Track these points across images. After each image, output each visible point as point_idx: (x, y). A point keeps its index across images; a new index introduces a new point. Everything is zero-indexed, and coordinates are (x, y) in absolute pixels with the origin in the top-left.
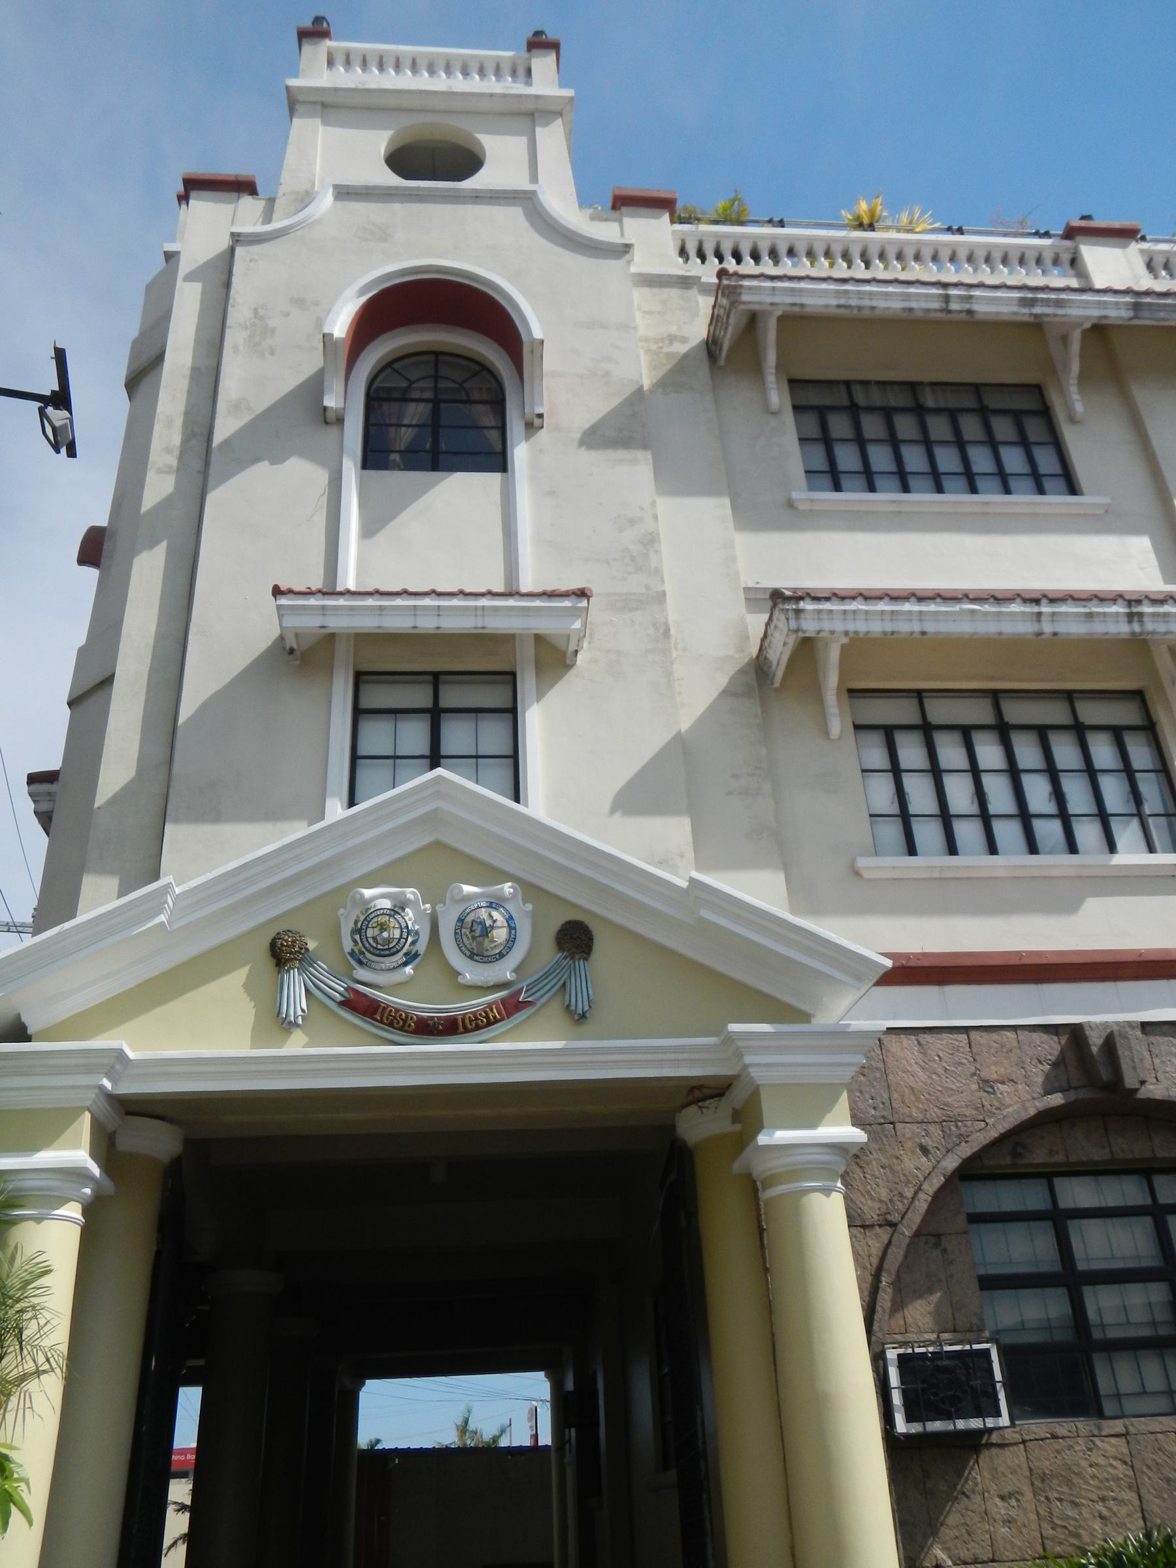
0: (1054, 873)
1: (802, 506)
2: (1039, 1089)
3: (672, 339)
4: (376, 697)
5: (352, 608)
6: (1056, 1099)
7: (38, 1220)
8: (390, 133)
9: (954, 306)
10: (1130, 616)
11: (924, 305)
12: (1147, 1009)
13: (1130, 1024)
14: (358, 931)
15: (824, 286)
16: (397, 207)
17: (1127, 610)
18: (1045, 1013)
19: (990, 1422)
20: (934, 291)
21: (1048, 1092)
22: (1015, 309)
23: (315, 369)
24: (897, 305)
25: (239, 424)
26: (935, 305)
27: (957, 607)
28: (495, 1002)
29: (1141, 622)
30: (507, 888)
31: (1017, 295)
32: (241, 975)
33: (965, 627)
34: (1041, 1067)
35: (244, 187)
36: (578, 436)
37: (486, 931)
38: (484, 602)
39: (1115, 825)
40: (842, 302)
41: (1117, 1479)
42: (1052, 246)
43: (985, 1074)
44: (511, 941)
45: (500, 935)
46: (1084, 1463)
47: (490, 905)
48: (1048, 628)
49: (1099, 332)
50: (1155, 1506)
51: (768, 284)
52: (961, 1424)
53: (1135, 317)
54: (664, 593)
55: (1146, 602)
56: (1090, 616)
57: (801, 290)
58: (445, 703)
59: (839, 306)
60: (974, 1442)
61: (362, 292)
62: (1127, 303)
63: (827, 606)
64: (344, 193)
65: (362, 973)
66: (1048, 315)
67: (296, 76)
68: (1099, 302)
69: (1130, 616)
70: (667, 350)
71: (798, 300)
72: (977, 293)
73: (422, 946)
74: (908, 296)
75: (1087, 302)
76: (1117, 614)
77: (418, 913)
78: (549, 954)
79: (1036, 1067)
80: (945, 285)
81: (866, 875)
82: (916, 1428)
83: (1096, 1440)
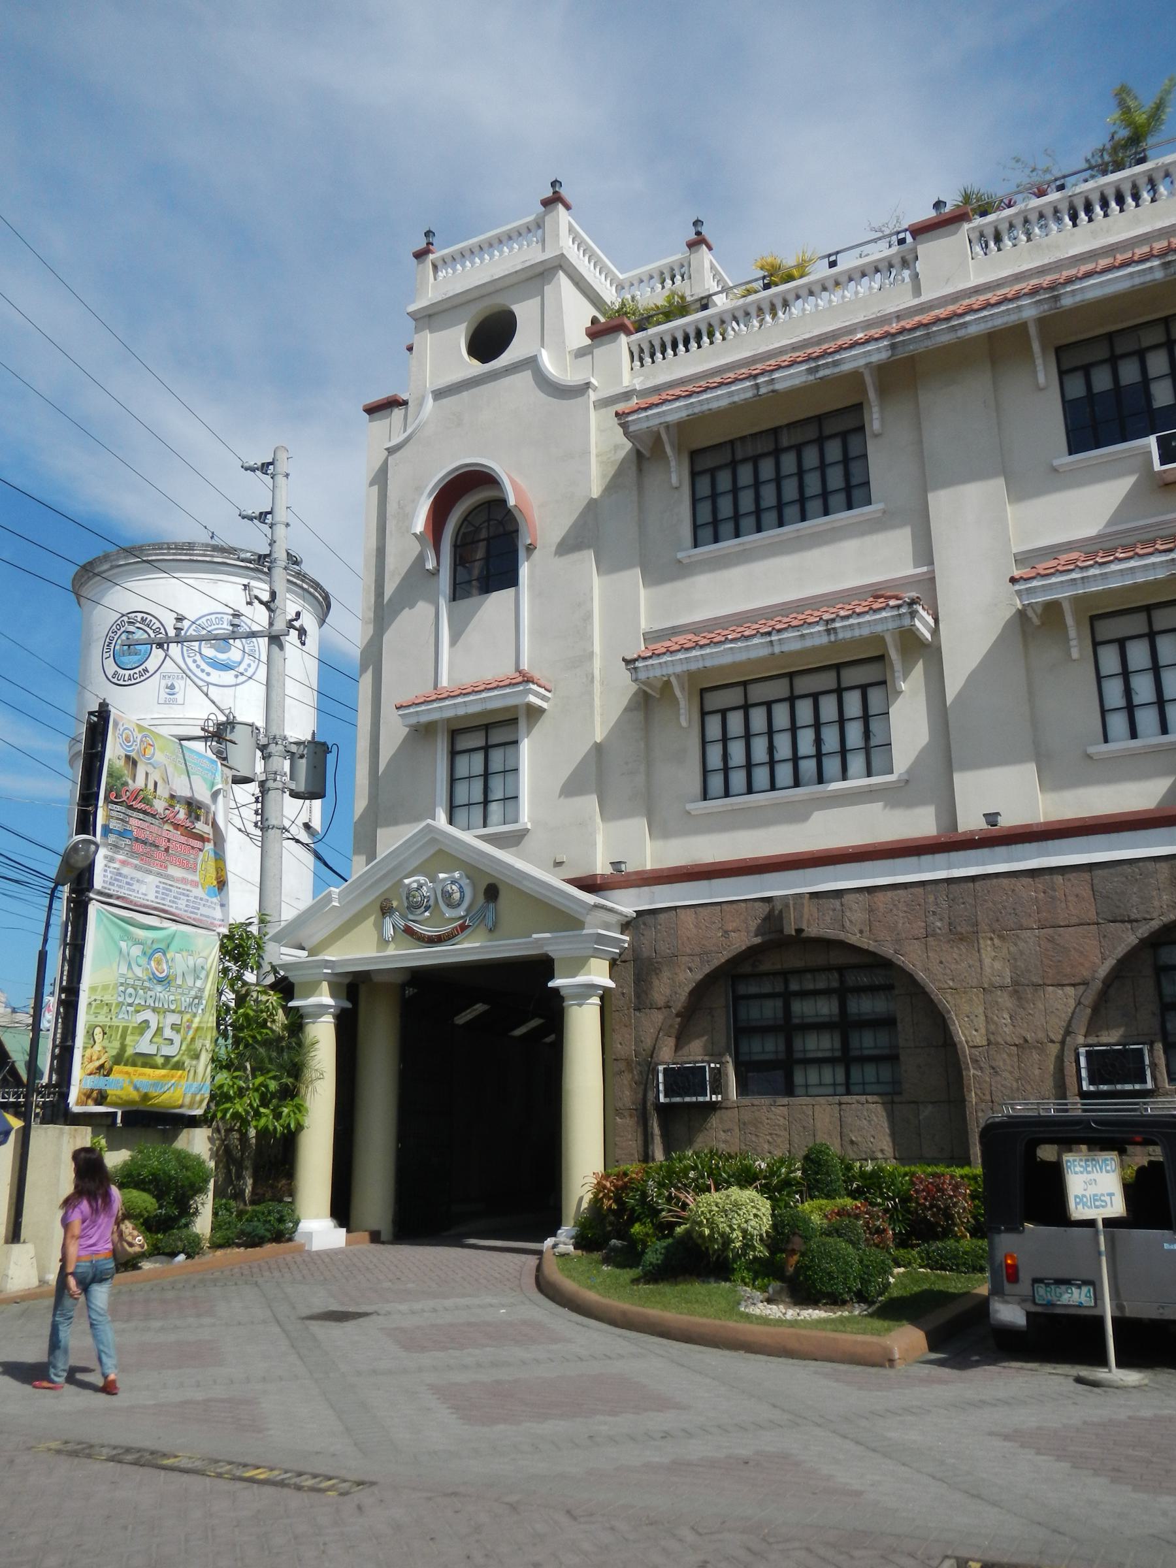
0: (796, 799)
1: (685, 562)
2: (752, 934)
3: (616, 448)
4: (464, 743)
5: (428, 710)
6: (758, 940)
7: (314, 1023)
8: (465, 325)
9: (763, 390)
10: (828, 631)
11: (743, 396)
14: (407, 898)
15: (677, 404)
16: (465, 395)
19: (701, 1099)
20: (748, 384)
21: (756, 936)
22: (803, 379)
23: (416, 553)
24: (724, 403)
25: (395, 586)
26: (749, 394)
28: (456, 927)
29: (836, 633)
30: (457, 875)
31: (804, 367)
32: (372, 919)
33: (727, 659)
35: (393, 403)
36: (554, 549)
37: (450, 895)
38: (484, 695)
39: (849, 757)
40: (690, 412)
41: (779, 1125)
42: (898, 252)
43: (724, 928)
44: (462, 898)
45: (457, 896)
46: (764, 1118)
47: (453, 882)
48: (777, 650)
50: (796, 1139)
51: (644, 414)
52: (687, 1099)
54: (592, 652)
56: (802, 636)
57: (664, 412)
58: (490, 743)
60: (713, 1107)
61: (430, 495)
62: (885, 346)
63: (650, 662)
64: (439, 394)
65: (411, 917)
67: (414, 302)
68: (864, 352)
69: (828, 631)
70: (612, 459)
71: (662, 420)
72: (776, 375)
73: (432, 902)
74: (731, 394)
77: (428, 888)
78: (481, 899)
80: (755, 377)
81: (693, 813)
82: (667, 1100)
83: (773, 1108)
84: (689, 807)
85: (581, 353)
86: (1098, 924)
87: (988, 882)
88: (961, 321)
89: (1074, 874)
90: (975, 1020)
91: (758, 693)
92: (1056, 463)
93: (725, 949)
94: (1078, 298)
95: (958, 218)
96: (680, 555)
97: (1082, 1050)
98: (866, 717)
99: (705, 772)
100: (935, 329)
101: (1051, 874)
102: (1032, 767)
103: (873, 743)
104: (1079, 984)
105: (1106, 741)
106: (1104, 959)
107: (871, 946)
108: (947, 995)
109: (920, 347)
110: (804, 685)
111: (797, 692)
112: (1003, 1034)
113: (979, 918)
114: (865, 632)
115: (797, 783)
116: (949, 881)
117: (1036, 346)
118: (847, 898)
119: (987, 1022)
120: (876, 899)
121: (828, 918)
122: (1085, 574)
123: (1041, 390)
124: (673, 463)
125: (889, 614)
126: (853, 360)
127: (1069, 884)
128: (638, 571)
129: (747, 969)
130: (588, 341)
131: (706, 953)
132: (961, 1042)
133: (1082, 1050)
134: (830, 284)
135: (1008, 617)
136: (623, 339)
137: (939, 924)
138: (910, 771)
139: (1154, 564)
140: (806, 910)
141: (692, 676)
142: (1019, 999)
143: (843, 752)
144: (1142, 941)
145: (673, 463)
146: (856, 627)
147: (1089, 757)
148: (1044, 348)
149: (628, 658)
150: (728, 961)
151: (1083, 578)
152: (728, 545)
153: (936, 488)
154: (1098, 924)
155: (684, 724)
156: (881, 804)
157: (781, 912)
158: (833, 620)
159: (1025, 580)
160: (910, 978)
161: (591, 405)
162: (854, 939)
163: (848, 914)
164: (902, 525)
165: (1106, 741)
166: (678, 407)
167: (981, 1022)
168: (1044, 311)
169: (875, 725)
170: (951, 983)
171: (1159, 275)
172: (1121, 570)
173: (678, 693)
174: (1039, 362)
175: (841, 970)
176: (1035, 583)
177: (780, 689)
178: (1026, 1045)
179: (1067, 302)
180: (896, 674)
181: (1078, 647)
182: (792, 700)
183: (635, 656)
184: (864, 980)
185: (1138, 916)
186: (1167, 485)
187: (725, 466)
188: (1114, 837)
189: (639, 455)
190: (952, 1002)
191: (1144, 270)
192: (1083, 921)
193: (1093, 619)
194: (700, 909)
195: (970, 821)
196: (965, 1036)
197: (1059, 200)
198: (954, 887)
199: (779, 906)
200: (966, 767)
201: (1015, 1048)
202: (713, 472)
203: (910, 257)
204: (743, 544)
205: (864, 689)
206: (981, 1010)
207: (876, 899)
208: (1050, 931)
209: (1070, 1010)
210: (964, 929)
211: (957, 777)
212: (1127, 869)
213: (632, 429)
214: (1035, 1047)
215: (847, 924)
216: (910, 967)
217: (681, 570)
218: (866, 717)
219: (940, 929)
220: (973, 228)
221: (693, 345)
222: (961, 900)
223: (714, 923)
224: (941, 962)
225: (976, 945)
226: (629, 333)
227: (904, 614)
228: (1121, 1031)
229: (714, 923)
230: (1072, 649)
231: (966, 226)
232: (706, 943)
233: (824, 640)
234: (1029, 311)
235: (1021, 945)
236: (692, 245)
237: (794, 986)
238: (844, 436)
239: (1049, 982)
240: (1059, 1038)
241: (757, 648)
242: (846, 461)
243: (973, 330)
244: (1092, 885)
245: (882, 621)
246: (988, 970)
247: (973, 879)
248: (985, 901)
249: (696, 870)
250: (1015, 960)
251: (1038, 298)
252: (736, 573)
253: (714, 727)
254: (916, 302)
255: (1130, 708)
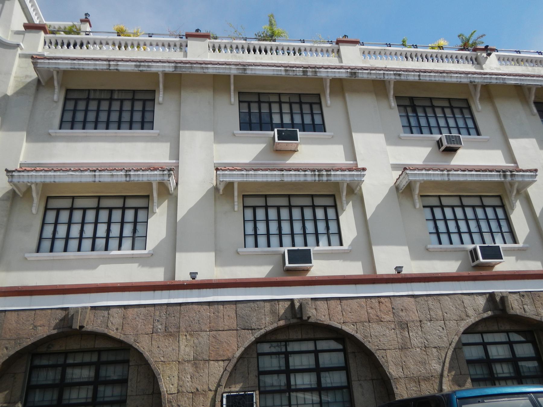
1: (52, 135)
3: (27, 76)
6: (55, 332)
9: (112, 68)
10: (126, 175)
11: (101, 67)
12: (96, 302)
13: (86, 308)
15: (66, 61)
17: (125, 173)
18: (63, 304)
20: (105, 63)
21: (54, 329)
22: (133, 68)
24: (91, 68)
26: (105, 67)
27: (67, 173)
31: (134, 64)
33: (68, 180)
34: (55, 321)
39: (124, 240)
40: (73, 67)
42: (179, 41)
43: (35, 324)
48: (97, 179)
49: (166, 75)
51: (47, 61)
53: (175, 71)
55: (132, 171)
56: (112, 175)
57: (58, 63)
59: (71, 68)
62: (173, 66)
63: (22, 174)
66: (144, 70)
68: (163, 66)
69: (126, 175)
71: (57, 66)
72: (120, 63)
74: (96, 65)
75: (159, 66)
76: (121, 175)
79: (54, 321)
81: (29, 259)
84: (27, 255)
85: (18, 33)
86: (237, 330)
87: (188, 306)
88: (206, 66)
89: (228, 305)
90: (173, 379)
91: (79, 203)
92: (235, 132)
93: (32, 336)
94: (253, 72)
95: (206, 36)
96: (50, 131)
97: (225, 395)
98: (135, 223)
99: (41, 239)
100: (195, 66)
101: (218, 305)
102: (213, 254)
103: (137, 235)
104: (226, 360)
105: (245, 247)
106: (238, 347)
107: (122, 337)
108: (160, 365)
109: (188, 71)
110: (105, 203)
111: (101, 206)
112: (186, 387)
113: (181, 325)
114: (145, 179)
115: (93, 249)
116: (168, 305)
117: (232, 88)
118: (112, 311)
119: (179, 380)
120: (128, 312)
121: (99, 321)
122: (248, 173)
123: (232, 105)
124: (57, 90)
125: (158, 173)
126: (156, 68)
127: (225, 310)
128: (25, 134)
129: (43, 349)
130: (23, 29)
131: (19, 339)
132: (163, 391)
133: (225, 395)
134: (148, 43)
135: (209, 188)
136: (42, 34)
137: (160, 327)
138: (154, 250)
139: (275, 174)
140: (88, 315)
141: (45, 186)
142: (196, 367)
143: (121, 237)
144: (256, 339)
145: (57, 90)
146: (141, 176)
147: (238, 253)
148: (234, 90)
149: (9, 169)
150: (32, 344)
151: (246, 174)
152: (78, 132)
153: (184, 129)
154: (237, 330)
155: (34, 211)
156: (137, 265)
157: (73, 315)
158: (130, 171)
159: (223, 170)
160: (140, 355)
161: (18, 55)
162: (112, 333)
163: (111, 319)
164: (166, 141)
165: (245, 247)
166: (67, 63)
167: (175, 380)
168: (240, 73)
169: (139, 227)
170: (162, 359)
171: (283, 73)
172: (262, 174)
173: (34, 195)
174: (232, 94)
175: (100, 351)
176: (226, 172)
177: (93, 203)
178: (198, 392)
179: (249, 72)
180: (155, 204)
181: (238, 206)
182: (98, 209)
183: (14, 169)
184: (112, 357)
185: (255, 327)
186: (277, 150)
187: (84, 99)
188: (248, 289)
189: (39, 81)
190: (161, 369)
191: (278, 70)
192: (230, 328)
193: (244, 196)
194: (22, 313)
195: (182, 276)
196: (166, 388)
197: (245, 44)
198: (170, 308)
199: (72, 312)
200: (182, 251)
201: (191, 394)
202: (76, 101)
203: (184, 44)
204: (86, 133)
205: (136, 209)
206: (176, 374)
207: (128, 312)
208: (215, 333)
209: (221, 374)
210: (172, 330)
211: (178, 255)
212: (252, 305)
213: (39, 66)
214: (202, 394)
215: (110, 325)
216: (141, 349)
217: (49, 138)
218: (135, 223)
219: (160, 329)
220: (211, 42)
221: (78, 47)
222: (173, 315)
223: (29, 321)
224: (158, 347)
225: (177, 338)
226: (46, 32)
227: (166, 174)
228: (242, 384)
229: (29, 321)
230: (235, 206)
231: (208, 40)
232: (20, 332)
233: (123, 179)
234: (234, 71)
235: (200, 339)
236: (82, 21)
237: (70, 361)
238: (144, 101)
239: (211, 359)
240: (213, 388)
241: (87, 177)
242: (144, 111)
243: (211, 71)
244: (236, 311)
245: (155, 176)
246: (182, 352)
247: (180, 304)
248: (185, 316)
249: (24, 289)
250: (197, 347)
251: (238, 67)
252: (80, 146)
253: (51, 217)
254: (185, 59)
255: (256, 235)
